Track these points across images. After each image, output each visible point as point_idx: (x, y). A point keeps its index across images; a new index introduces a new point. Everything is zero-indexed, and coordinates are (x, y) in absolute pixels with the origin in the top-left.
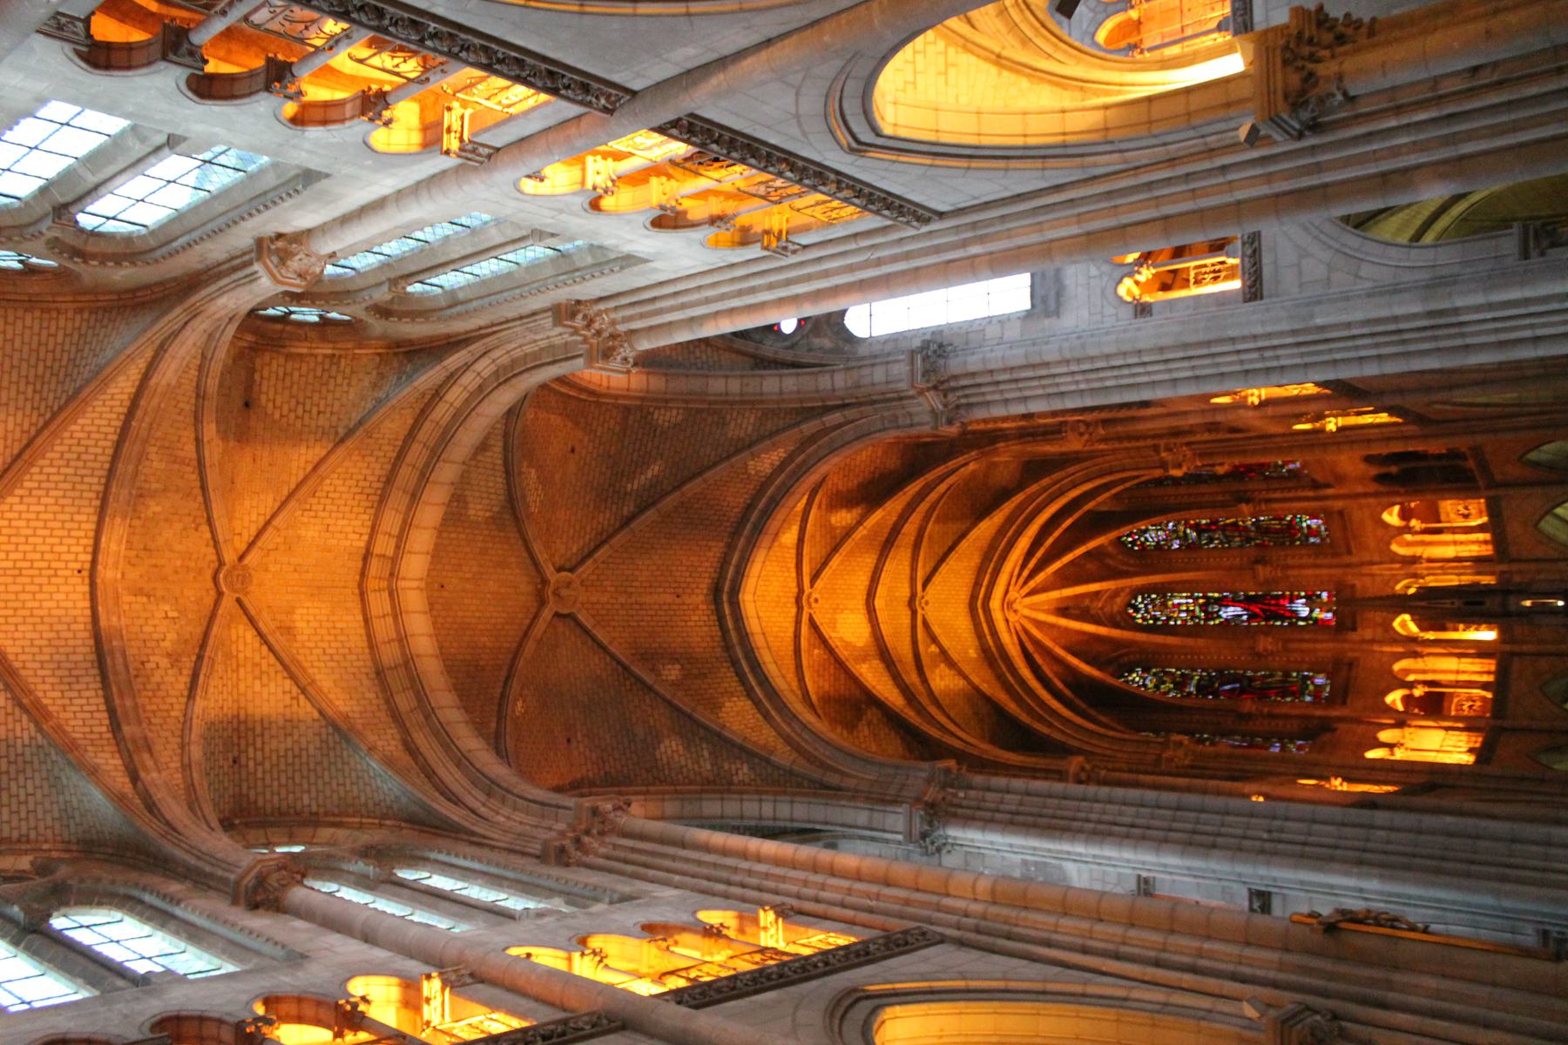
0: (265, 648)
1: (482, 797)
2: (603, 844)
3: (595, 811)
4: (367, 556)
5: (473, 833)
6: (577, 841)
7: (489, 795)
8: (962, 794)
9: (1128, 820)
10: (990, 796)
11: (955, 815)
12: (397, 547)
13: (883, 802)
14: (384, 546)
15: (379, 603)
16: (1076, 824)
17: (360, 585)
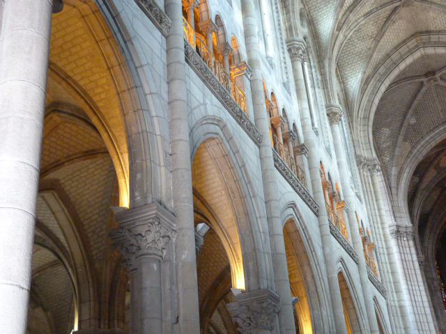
0: (385, 19)
1: (362, 117)
2: (366, 172)
3: (375, 165)
4: (428, 32)
5: (352, 122)
6: (365, 164)
7: (364, 118)
8: (405, 239)
9: (416, 300)
10: (408, 249)
11: (398, 240)
12: (435, 42)
13: (394, 212)
14: (434, 38)
15: (412, 43)
16: (409, 283)
17: (416, 33)
